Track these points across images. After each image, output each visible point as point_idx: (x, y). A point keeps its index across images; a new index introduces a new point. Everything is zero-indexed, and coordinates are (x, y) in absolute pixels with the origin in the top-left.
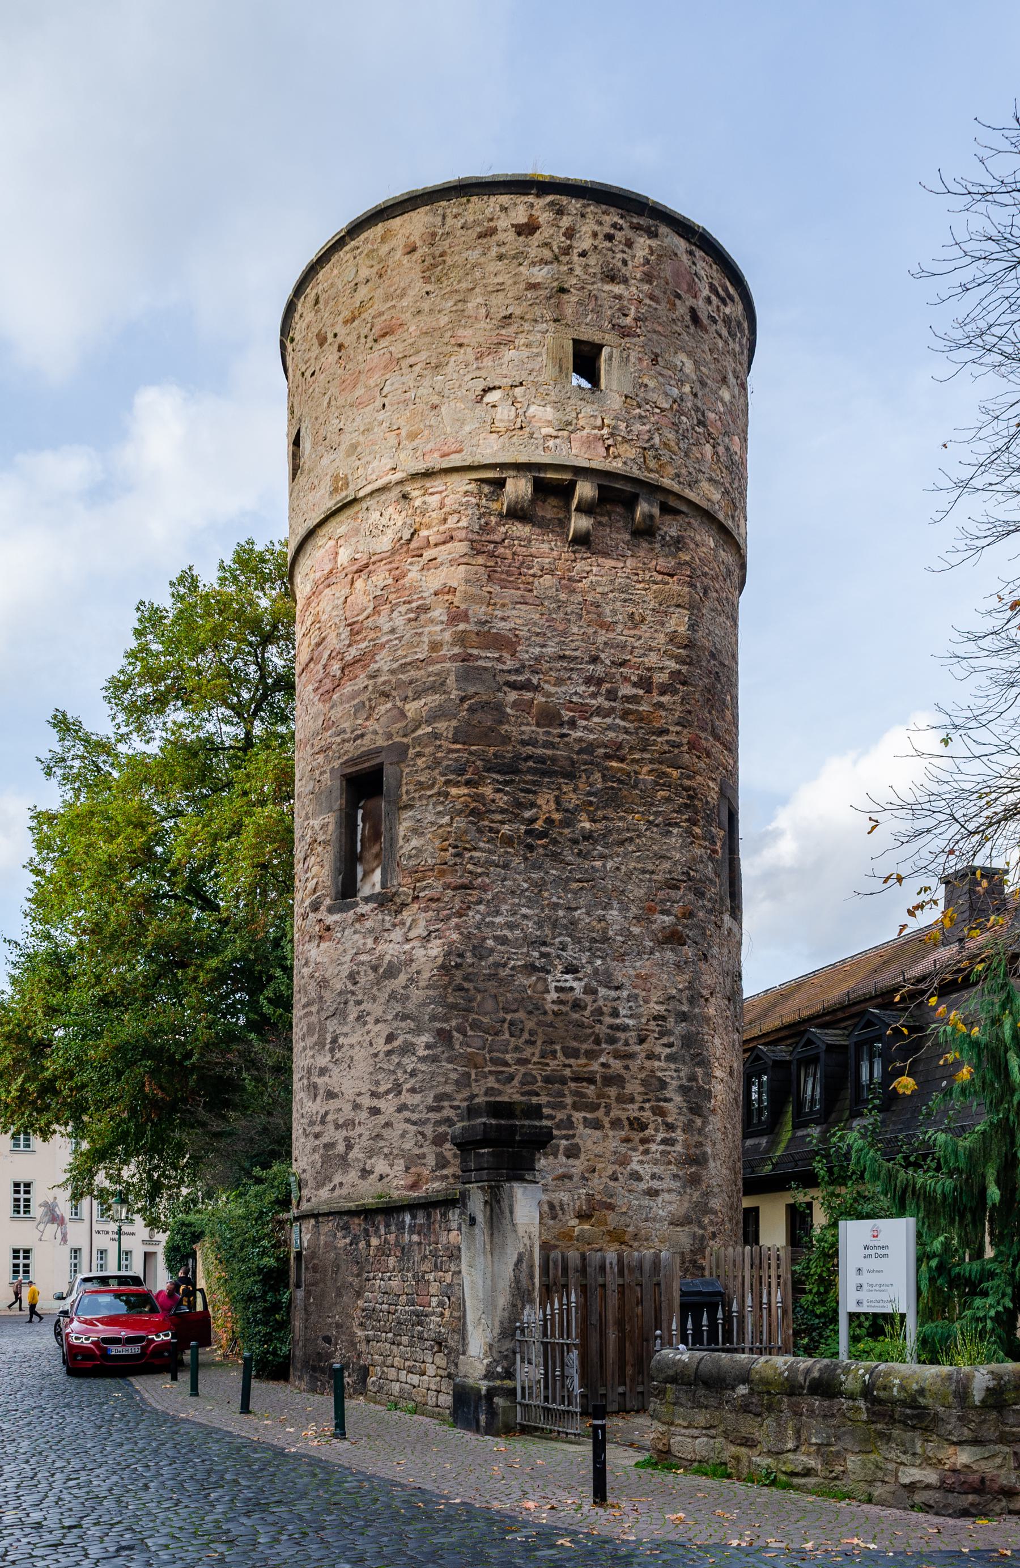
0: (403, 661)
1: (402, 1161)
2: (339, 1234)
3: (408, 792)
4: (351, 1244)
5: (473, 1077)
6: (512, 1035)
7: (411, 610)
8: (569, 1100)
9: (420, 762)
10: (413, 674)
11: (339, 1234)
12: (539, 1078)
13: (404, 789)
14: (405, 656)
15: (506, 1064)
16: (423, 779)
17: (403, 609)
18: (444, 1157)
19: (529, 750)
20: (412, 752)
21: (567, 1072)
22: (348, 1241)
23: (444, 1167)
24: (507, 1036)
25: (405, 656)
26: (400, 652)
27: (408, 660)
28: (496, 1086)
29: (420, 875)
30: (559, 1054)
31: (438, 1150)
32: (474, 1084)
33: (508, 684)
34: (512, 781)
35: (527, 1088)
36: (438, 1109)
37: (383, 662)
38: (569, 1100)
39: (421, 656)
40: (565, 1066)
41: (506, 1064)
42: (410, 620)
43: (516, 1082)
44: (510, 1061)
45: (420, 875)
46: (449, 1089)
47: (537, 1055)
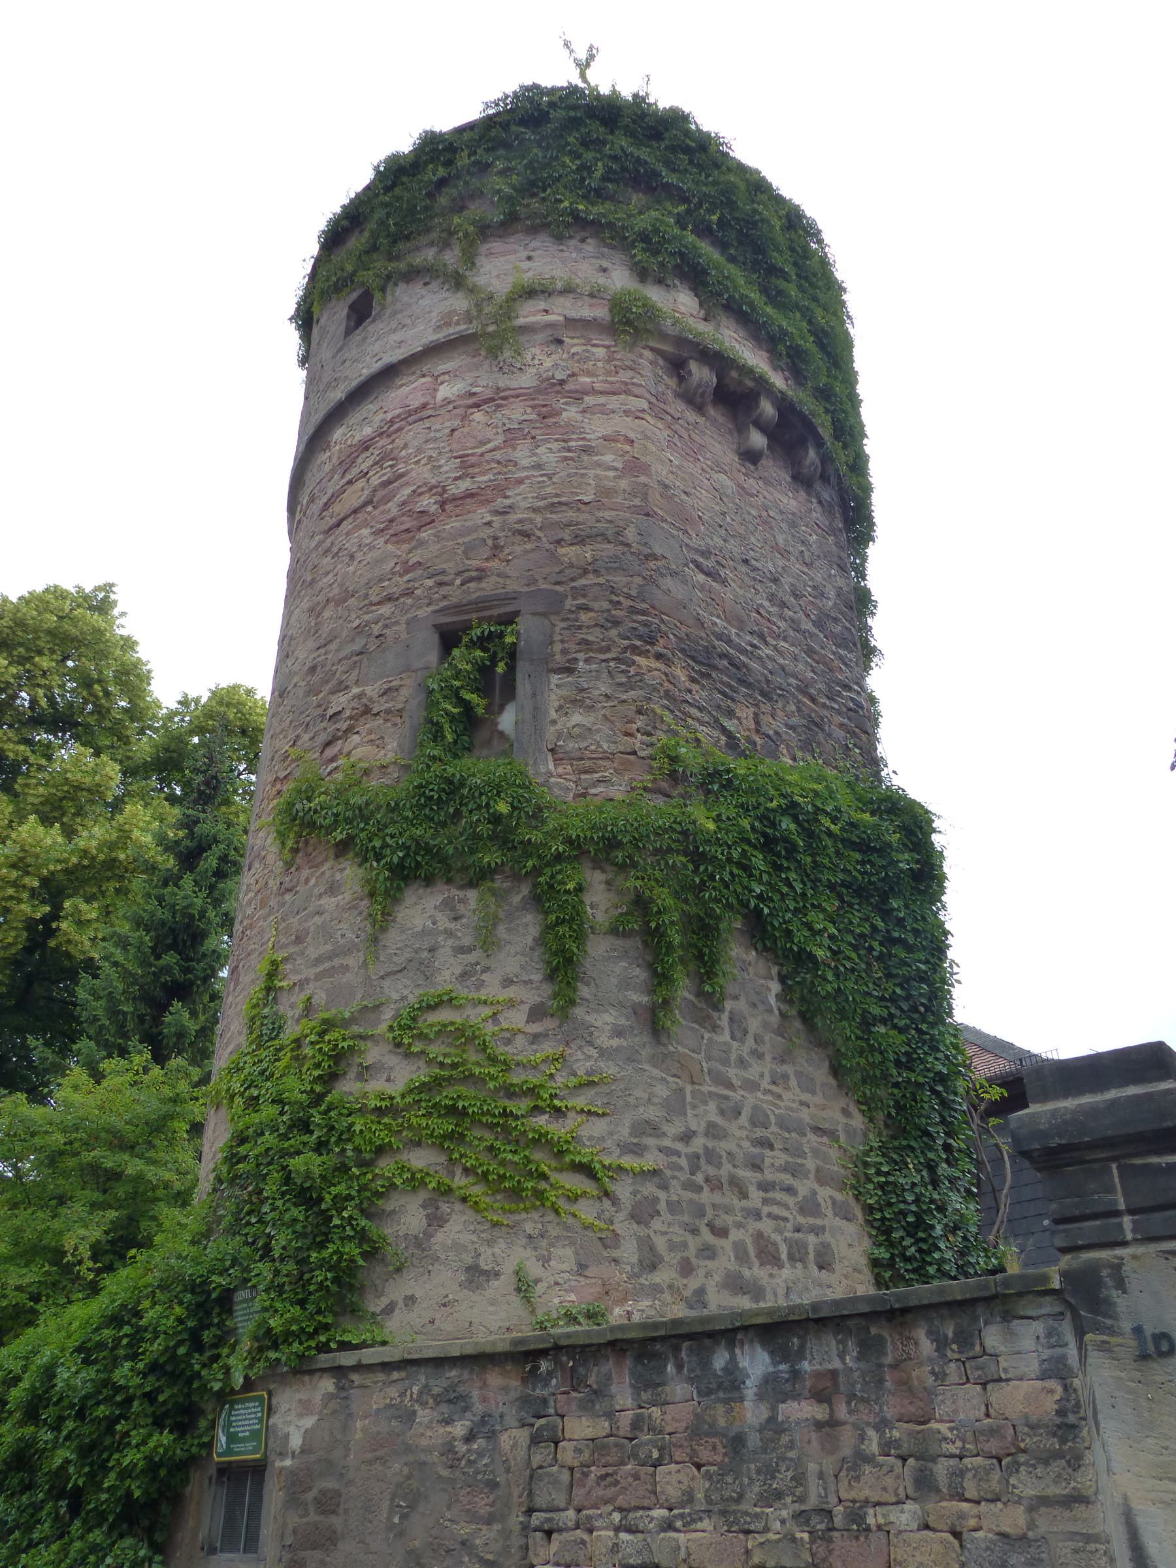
0: (556, 500)
1: (569, 1252)
2: (424, 1415)
3: (564, 652)
4: (469, 1438)
5: (689, 1098)
6: (733, 1038)
7: (569, 450)
8: (810, 1164)
9: (584, 617)
10: (570, 515)
11: (424, 1415)
12: (772, 1118)
13: (557, 647)
14: (557, 495)
15: (730, 1086)
16: (590, 638)
17: (555, 446)
18: (652, 1248)
19: (722, 646)
20: (569, 603)
21: (805, 1115)
22: (459, 1429)
23: (653, 1267)
24: (726, 1037)
25: (557, 495)
26: (549, 490)
27: (563, 499)
28: (719, 1120)
29: (588, 763)
30: (793, 1082)
31: (642, 1231)
32: (689, 1112)
33: (694, 561)
34: (709, 676)
35: (759, 1133)
36: (637, 1150)
37: (522, 497)
38: (810, 1164)
39: (586, 499)
40: (802, 1103)
41: (730, 1086)
42: (566, 459)
43: (744, 1119)
44: (734, 1081)
45: (588, 763)
46: (652, 1113)
47: (767, 1078)
